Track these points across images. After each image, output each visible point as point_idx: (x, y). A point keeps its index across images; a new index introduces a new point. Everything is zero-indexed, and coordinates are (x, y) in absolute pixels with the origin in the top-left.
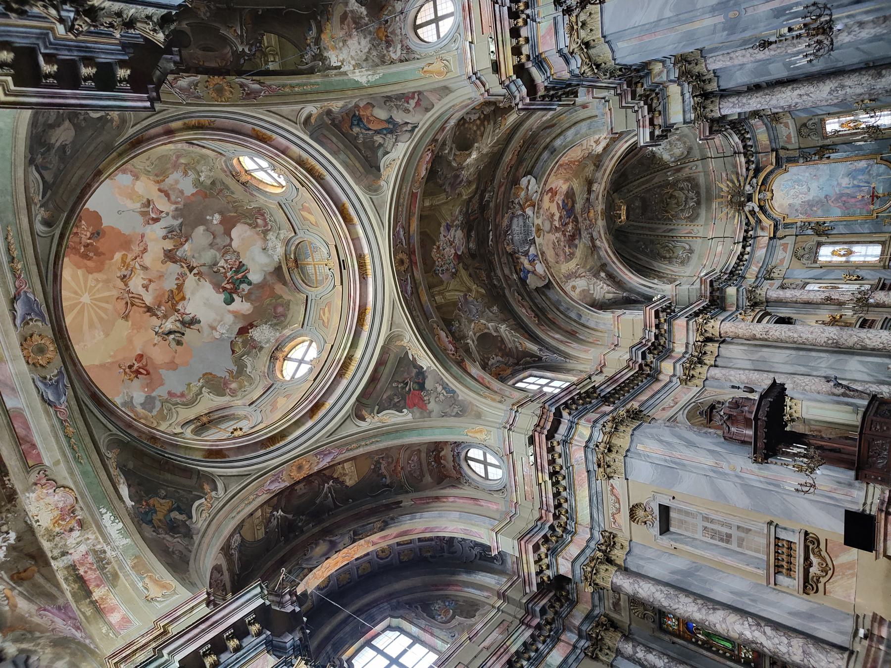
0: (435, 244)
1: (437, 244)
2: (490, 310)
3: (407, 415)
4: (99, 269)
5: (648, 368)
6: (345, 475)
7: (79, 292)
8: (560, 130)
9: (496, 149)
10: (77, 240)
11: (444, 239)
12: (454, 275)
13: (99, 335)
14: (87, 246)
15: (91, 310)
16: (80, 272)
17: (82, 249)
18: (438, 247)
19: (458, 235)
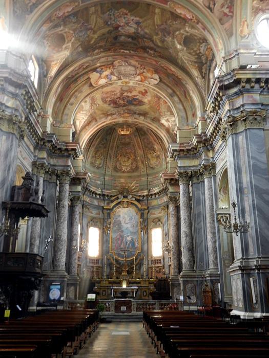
0: (129, 12)
1: (129, 14)
2: (80, 45)
5: (42, 143)
8: (183, 100)
9: (179, 61)
11: (131, 19)
12: (106, 23)
18: (127, 14)
19: (131, 30)
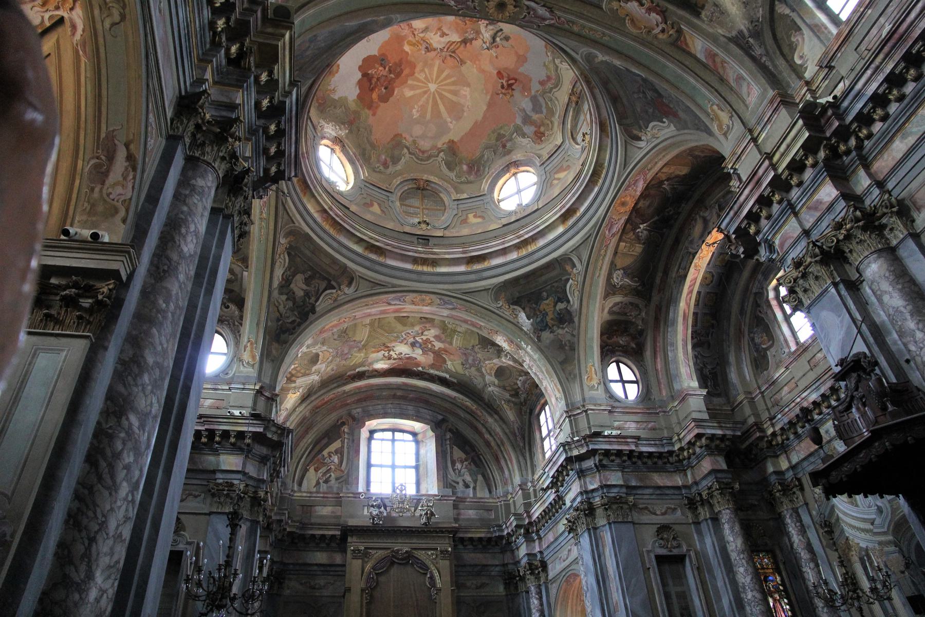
3: (668, 126)
4: (413, 66)
6: (671, 174)
7: (426, 89)
10: (383, 79)
13: (465, 91)
14: (390, 72)
15: (444, 87)
16: (410, 82)
17: (392, 76)
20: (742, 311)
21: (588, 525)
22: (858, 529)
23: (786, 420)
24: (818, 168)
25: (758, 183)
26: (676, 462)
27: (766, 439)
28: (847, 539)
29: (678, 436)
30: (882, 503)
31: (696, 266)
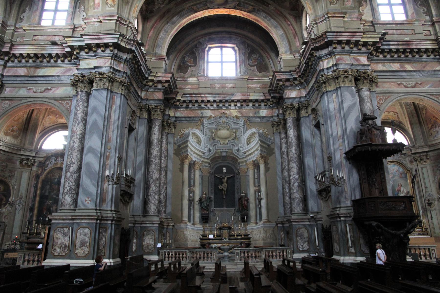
20: (187, 44)
21: (108, 87)
22: (195, 153)
23: (190, 99)
24: (368, 51)
25: (353, 36)
26: (144, 84)
27: (174, 100)
28: (187, 154)
29: (156, 74)
30: (213, 149)
31: (204, 13)
